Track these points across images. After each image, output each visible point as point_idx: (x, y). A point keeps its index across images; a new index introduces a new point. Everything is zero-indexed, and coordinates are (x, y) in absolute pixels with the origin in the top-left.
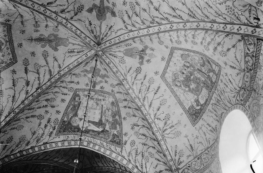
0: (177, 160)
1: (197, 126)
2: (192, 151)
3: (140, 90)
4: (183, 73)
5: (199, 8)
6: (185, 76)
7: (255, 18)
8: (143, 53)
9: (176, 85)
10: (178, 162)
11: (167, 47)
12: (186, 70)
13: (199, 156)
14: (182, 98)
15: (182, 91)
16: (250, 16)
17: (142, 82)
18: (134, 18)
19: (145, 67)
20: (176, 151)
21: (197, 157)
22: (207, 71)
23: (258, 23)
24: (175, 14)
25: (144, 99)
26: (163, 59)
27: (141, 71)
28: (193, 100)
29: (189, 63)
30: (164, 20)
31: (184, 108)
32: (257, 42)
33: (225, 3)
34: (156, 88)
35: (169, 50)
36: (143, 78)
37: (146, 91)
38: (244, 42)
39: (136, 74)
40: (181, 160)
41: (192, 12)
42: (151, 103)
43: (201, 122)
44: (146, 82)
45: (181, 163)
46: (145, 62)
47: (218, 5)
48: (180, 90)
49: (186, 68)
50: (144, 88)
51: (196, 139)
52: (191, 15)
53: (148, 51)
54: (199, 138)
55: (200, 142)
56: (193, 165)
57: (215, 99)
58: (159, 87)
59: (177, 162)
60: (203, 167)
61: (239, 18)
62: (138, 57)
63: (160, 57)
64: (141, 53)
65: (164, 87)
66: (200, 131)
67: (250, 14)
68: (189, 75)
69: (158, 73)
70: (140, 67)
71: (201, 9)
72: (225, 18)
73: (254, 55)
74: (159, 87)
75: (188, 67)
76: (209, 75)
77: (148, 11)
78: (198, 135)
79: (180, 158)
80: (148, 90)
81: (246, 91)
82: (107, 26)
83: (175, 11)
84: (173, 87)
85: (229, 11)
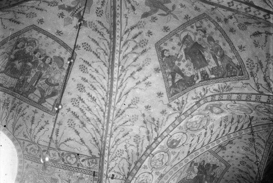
4: (35, 53)
5: (124, 124)
6: (30, 54)
7: (113, 175)
8: (76, 13)
9: (18, 43)
16: (115, 172)
18: (132, 44)
22: (40, 86)
23: (109, 177)
24: (123, 94)
26: (59, 32)
29: (50, 63)
30: (121, 82)
32: (91, 171)
33: (126, 151)
38: (89, 157)
41: (121, 114)
47: (124, 144)
48: (12, 48)
49: (42, 58)
52: (119, 112)
61: (113, 160)
62: (73, 6)
63: (63, 29)
67: (117, 172)
68: (33, 61)
71: (123, 125)
72: (113, 147)
73: (80, 167)
75: (44, 61)
76: (35, 89)
77: (134, 63)
81: (38, 152)
82: (138, 4)
83: (126, 94)
84: (16, 38)
85: (119, 153)
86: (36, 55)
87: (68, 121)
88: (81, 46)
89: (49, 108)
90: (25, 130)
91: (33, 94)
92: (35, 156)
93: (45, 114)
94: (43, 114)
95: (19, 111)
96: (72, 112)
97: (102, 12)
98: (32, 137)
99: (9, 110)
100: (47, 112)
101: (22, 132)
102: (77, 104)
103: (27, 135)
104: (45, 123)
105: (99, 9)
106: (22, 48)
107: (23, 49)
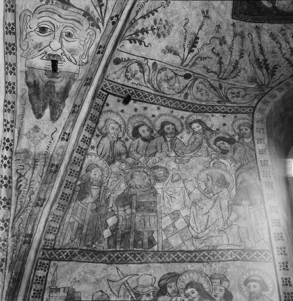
0: (139, 27)
2: (187, 50)
10: (136, 33)
13: (192, 74)
20: (157, 11)
21: (187, 72)
40: (149, 38)
43: (249, 26)
45: (140, 42)
51: (217, 42)
54: (225, 48)
55: (218, 55)
56: (163, 73)
59: (134, 30)
60: (182, 98)
78: (229, 40)
79: (150, 32)
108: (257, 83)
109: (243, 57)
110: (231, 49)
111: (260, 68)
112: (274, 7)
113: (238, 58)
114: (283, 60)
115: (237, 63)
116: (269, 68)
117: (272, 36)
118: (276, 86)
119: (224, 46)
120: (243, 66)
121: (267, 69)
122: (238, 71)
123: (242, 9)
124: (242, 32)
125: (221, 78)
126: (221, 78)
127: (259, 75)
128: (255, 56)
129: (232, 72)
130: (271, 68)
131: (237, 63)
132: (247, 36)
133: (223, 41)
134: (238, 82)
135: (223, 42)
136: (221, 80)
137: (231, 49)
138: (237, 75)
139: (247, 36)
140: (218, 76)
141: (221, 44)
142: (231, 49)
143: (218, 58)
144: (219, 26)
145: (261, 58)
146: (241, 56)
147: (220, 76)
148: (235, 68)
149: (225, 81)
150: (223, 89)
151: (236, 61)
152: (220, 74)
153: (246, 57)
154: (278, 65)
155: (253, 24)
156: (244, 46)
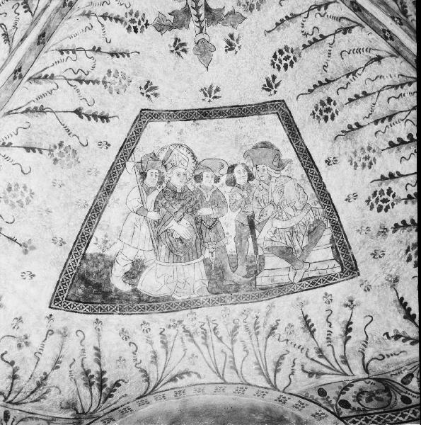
1: (63, 318)
3: (74, 51)
4: (198, 178)
6: (192, 188)
8: (202, 18)
9: (144, 175)
11: (270, 85)
12: (217, 180)
14: (112, 215)
15: (135, 204)
17: (99, 49)
19: (155, 44)
22: (269, 244)
25: (46, 76)
26: (209, 92)
27: (136, 31)
28: (131, 254)
29: (251, 177)
31: (84, 239)
34: (98, 109)
35: (264, 97)
36: (115, 46)
37: (76, 76)
39: (122, 15)
42: (42, 110)
44: (104, 64)
46: (169, 37)
49: (223, 179)
50: (83, 62)
51: (14, 343)
53: (217, 34)
54: (27, 352)
55: (12, 363)
57: (203, 320)
58: (105, 118)
63: (208, 80)
64: (202, 11)
65: (116, 133)
66: (55, 338)
68: (208, 199)
69: (152, 97)
70: (147, 24)
74: (105, 118)
75: (232, 183)
76: (262, 258)
78: (36, 341)
80: (80, 81)
86: (208, 181)
87: (407, 256)
88: (275, 72)
89: (329, 272)
90: (301, 358)
91: (265, 273)
92: (387, 409)
93: (329, 289)
94: (326, 294)
95: (256, 329)
96: (397, 226)
97: (371, 164)
98: (337, 367)
99: (227, 340)
100: (331, 282)
101: (298, 368)
102: (391, 198)
103: (317, 367)
104: (348, 310)
105: (288, 51)
106: (160, 183)
107: (164, 185)
108: (76, 409)
109: (58, 367)
110: (38, 355)
111: (89, 384)
112: (135, 291)
113: (48, 370)
114: (136, 371)
115: (46, 377)
116: (105, 385)
117: (125, 335)
118: (105, 414)
119: (25, 348)
120: (56, 383)
121: (101, 387)
122: (45, 390)
123: (73, 295)
124: (65, 329)
125: (10, 402)
126: (10, 402)
127: (82, 397)
128: (82, 365)
129: (32, 393)
130: (109, 386)
131: (46, 377)
132: (73, 334)
133: (24, 342)
134: (41, 408)
135: (23, 344)
136: (10, 405)
137: (37, 354)
138: (42, 397)
139: (73, 334)
140: (6, 399)
141: (20, 346)
142: (37, 354)
143: (11, 369)
144: (20, 320)
145: (94, 369)
146: (56, 367)
147: (10, 399)
148: (39, 385)
149: (16, 407)
150: (11, 420)
151: (45, 373)
152: (9, 395)
153: (64, 367)
154: (123, 381)
155: (93, 317)
156: (63, 350)
